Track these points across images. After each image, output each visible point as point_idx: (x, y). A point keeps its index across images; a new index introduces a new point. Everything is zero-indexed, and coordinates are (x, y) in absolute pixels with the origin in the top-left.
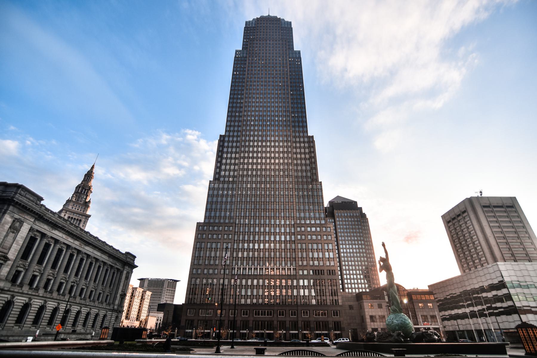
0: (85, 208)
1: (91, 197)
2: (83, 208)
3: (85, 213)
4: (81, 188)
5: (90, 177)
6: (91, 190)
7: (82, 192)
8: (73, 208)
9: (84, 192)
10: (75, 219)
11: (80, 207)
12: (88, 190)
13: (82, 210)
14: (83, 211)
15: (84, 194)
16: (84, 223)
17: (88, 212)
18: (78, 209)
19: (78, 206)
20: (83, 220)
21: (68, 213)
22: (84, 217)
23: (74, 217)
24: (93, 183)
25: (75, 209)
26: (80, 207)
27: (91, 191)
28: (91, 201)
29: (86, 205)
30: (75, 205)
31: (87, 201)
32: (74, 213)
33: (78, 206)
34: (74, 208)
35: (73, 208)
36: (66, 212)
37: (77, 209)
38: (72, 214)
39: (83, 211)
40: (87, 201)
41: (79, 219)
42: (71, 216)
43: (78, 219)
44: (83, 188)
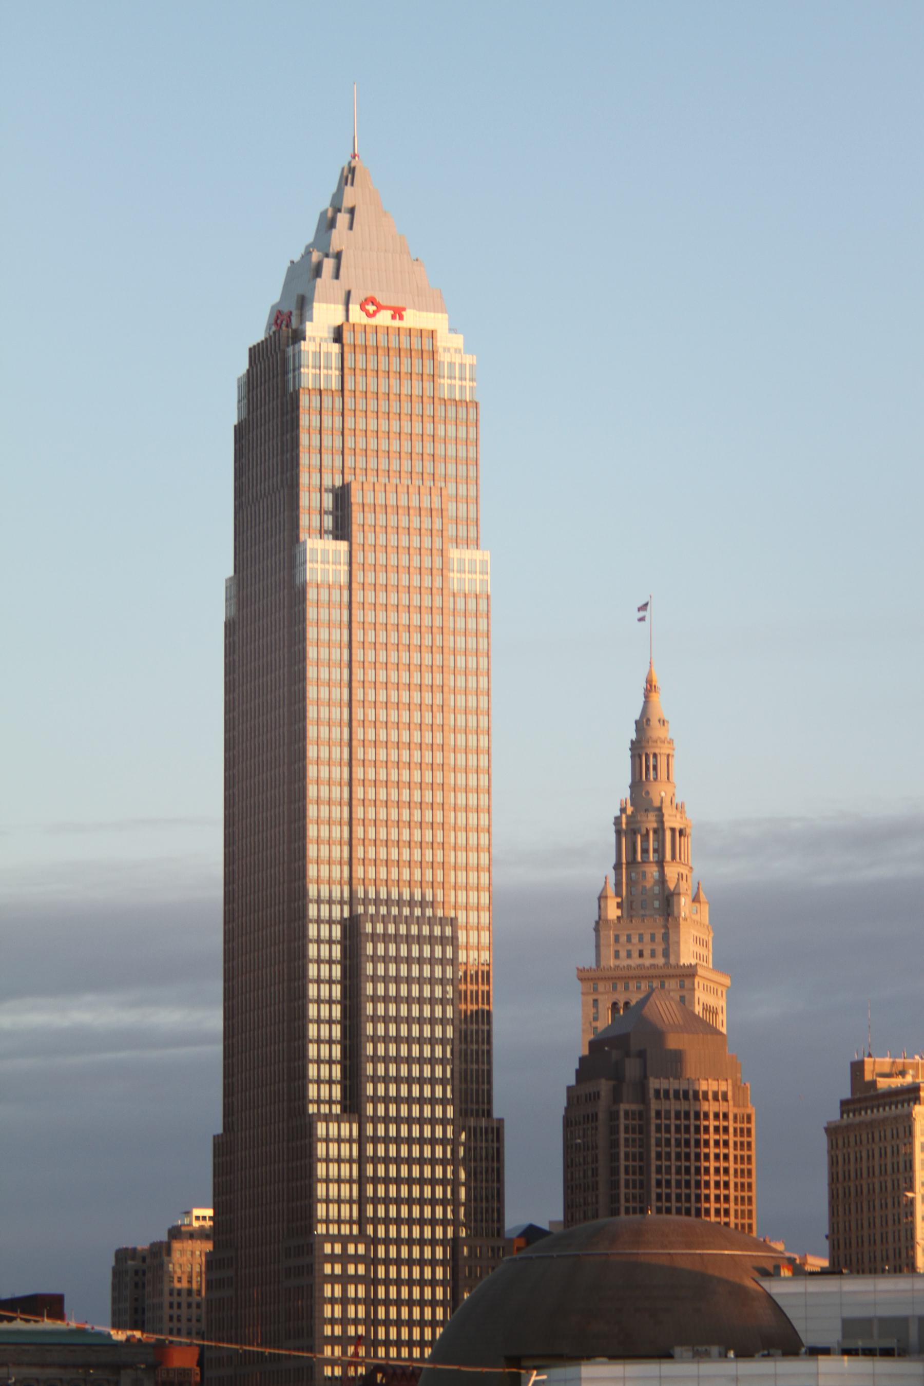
0: (666, 937)
5: (647, 756)
6: (667, 825)
11: (647, 938)
12: (656, 831)
18: (641, 955)
19: (635, 940)
21: (601, 987)
25: (629, 955)
26: (647, 938)
27: (673, 830)
30: (623, 939)
32: (626, 979)
33: (635, 940)
34: (623, 954)
37: (635, 954)
39: (666, 954)
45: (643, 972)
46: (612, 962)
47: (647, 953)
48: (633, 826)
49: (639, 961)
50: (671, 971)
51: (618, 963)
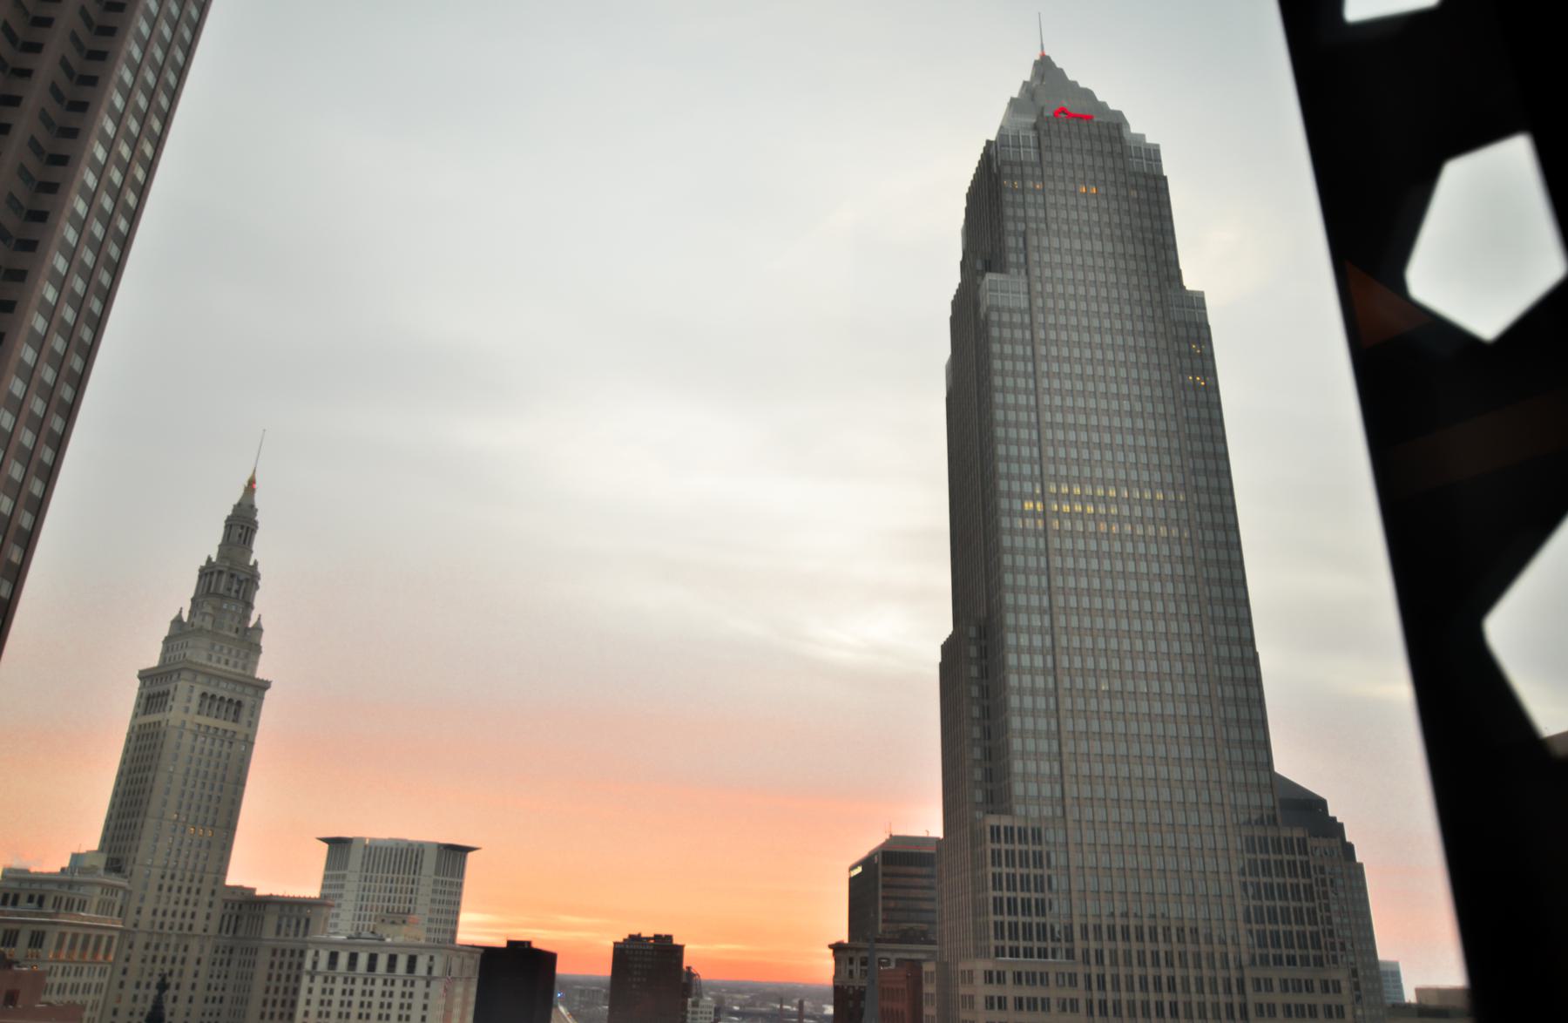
0: (247, 656)
1: (265, 606)
2: (242, 654)
3: (248, 673)
4: (224, 577)
7: (229, 589)
8: (210, 658)
9: (237, 592)
10: (222, 699)
11: (234, 652)
13: (240, 663)
14: (244, 668)
15: (237, 598)
16: (252, 715)
17: (261, 673)
18: (227, 663)
19: (225, 651)
20: (248, 701)
22: (249, 690)
23: (219, 694)
24: (262, 551)
26: (234, 652)
28: (264, 624)
29: (249, 641)
30: (217, 648)
31: (251, 624)
33: (225, 651)
34: (214, 658)
35: (210, 658)
36: (194, 680)
37: (223, 661)
38: (213, 682)
39: (244, 668)
40: (251, 624)
41: (236, 698)
42: (210, 691)
43: (230, 701)
44: (232, 576)
45: (229, 676)
46: (204, 662)
47: (231, 662)
48: (233, 572)
49: (224, 667)
50: (249, 681)
51: (209, 664)
